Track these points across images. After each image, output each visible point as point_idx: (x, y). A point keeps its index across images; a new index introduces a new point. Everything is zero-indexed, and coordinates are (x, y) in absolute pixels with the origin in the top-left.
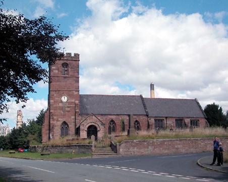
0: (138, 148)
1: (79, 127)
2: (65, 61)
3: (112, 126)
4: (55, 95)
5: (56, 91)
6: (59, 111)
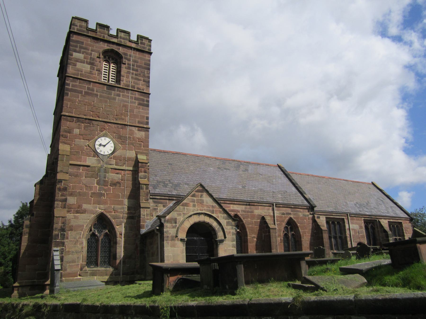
2: (115, 47)
4: (77, 131)
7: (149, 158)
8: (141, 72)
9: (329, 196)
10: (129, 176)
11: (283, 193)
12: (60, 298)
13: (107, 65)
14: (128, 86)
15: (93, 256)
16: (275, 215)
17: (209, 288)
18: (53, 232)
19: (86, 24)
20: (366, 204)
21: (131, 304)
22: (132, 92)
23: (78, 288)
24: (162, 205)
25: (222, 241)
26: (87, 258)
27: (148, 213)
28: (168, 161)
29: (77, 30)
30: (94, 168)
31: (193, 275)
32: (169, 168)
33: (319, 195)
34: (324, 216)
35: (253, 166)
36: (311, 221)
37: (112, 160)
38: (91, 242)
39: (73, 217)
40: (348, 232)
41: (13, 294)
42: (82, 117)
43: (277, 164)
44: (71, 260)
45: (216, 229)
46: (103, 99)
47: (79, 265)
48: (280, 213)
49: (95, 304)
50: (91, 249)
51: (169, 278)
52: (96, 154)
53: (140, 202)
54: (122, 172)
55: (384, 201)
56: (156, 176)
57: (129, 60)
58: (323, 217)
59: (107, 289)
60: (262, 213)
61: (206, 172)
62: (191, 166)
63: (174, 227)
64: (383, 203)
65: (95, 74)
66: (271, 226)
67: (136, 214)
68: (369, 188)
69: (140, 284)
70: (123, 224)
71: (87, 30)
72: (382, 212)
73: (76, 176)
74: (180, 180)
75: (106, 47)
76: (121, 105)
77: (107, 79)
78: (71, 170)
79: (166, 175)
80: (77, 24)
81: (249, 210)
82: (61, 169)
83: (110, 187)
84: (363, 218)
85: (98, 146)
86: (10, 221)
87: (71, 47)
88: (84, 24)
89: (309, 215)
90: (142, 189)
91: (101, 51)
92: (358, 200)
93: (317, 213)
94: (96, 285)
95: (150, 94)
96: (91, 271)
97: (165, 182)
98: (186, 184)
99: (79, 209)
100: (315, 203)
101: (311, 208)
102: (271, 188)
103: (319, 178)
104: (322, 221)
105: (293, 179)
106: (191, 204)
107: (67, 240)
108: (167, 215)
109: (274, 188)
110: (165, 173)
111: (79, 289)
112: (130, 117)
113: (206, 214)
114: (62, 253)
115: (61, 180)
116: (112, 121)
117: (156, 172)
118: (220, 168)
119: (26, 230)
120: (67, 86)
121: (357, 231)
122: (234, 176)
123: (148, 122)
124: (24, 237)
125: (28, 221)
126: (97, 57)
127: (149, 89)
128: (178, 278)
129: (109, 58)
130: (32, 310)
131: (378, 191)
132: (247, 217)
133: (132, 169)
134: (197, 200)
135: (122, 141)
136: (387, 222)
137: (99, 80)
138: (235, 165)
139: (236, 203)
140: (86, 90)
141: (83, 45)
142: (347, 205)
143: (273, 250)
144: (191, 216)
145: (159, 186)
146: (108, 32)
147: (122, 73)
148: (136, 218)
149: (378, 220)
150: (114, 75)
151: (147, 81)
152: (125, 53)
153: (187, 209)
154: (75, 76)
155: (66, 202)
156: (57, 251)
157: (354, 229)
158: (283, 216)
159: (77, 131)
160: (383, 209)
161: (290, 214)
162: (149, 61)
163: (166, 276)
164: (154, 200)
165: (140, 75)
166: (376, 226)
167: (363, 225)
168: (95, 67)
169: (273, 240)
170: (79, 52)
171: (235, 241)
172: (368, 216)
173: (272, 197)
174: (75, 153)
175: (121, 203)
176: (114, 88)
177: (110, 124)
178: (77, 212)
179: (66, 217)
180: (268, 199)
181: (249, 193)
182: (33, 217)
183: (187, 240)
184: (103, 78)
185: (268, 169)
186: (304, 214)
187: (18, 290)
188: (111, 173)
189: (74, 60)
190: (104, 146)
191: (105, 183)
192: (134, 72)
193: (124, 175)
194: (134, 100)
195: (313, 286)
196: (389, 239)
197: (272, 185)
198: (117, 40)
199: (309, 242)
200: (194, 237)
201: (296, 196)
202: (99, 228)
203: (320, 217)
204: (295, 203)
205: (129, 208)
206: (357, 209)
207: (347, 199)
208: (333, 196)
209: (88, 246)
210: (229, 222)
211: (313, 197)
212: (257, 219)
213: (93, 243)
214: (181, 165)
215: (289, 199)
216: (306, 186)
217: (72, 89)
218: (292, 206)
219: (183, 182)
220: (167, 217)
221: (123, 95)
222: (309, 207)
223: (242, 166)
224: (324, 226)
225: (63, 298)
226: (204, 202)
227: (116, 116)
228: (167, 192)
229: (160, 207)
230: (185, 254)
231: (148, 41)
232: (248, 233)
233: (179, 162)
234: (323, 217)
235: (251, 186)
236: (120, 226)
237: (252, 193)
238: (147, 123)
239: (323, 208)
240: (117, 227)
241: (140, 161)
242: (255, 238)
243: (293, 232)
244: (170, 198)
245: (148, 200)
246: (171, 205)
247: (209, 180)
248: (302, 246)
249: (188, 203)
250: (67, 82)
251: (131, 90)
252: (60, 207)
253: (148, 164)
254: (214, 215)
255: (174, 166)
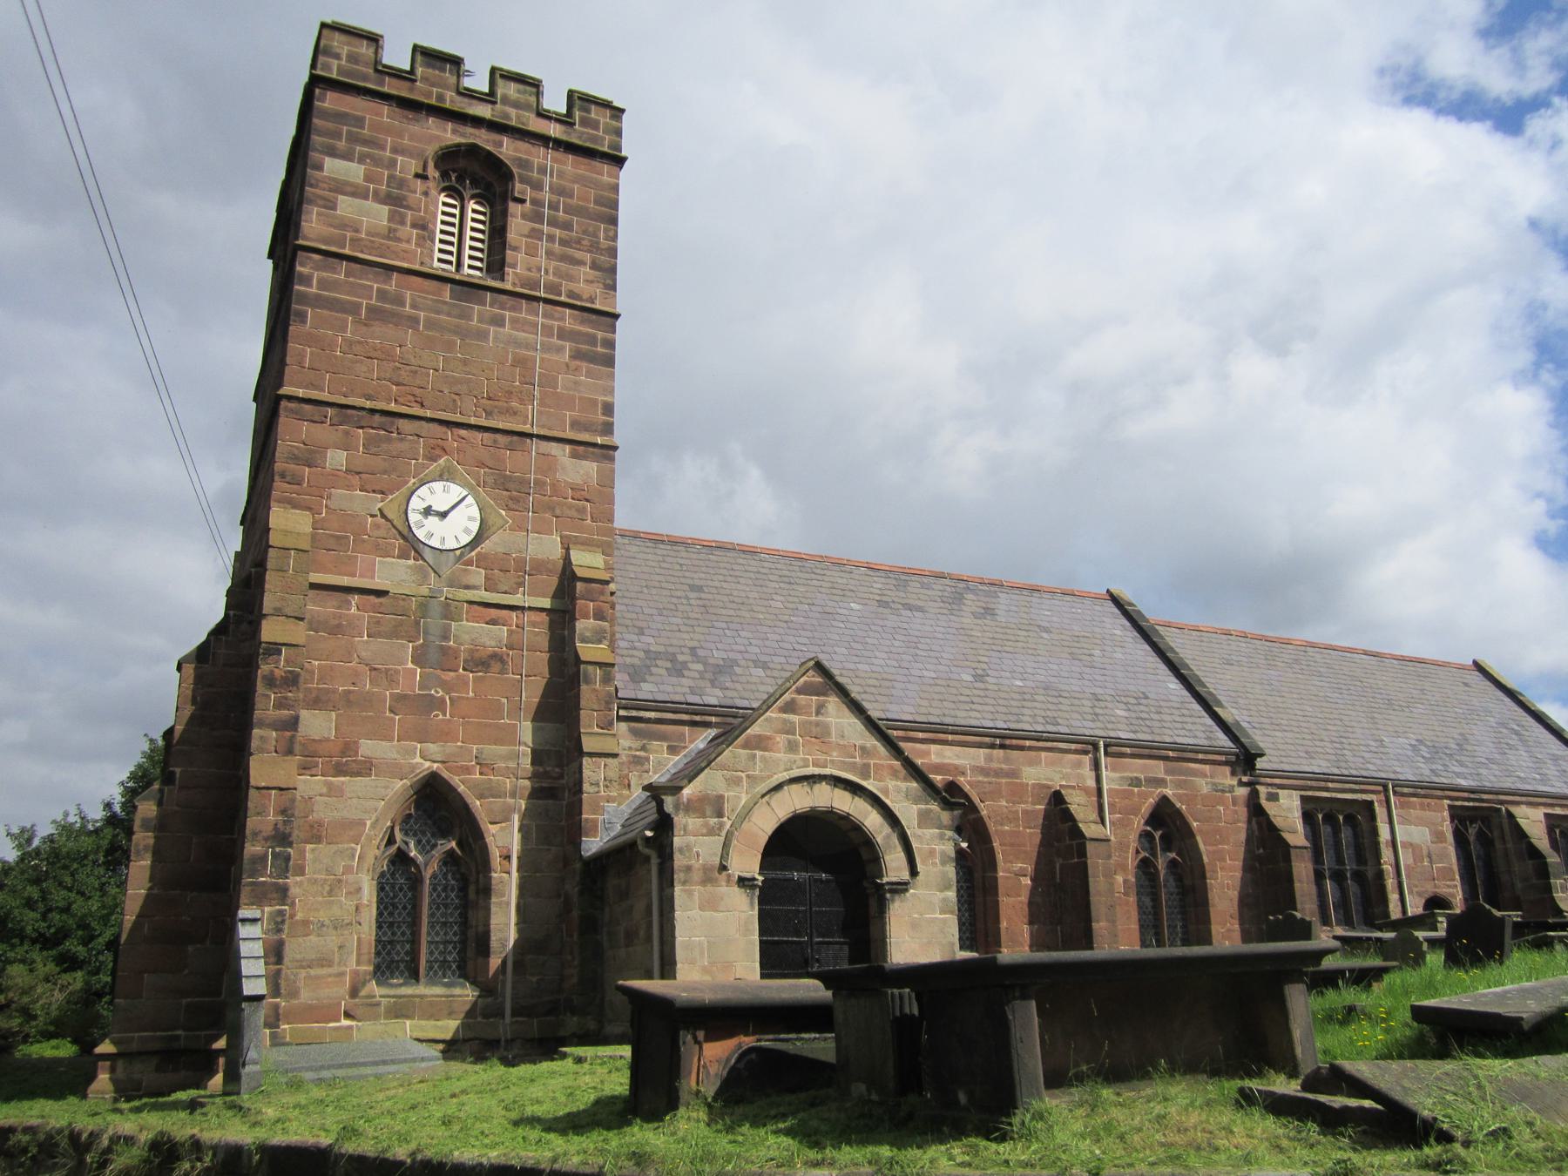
2: (483, 139)
4: (337, 458)
7: (615, 566)
8: (585, 232)
9: (1310, 714)
10: (537, 632)
11: (1133, 701)
12: (259, 1112)
13: (454, 206)
14: (536, 286)
15: (398, 942)
16: (1105, 787)
17: (874, 1097)
18: (243, 848)
19: (371, 51)
20: (1458, 745)
21: (538, 1162)
22: (549, 307)
23: (334, 1071)
24: (665, 745)
25: (900, 888)
26: (376, 946)
27: (613, 774)
28: (687, 574)
29: (340, 71)
30: (404, 600)
31: (804, 1035)
32: (693, 602)
33: (1272, 710)
34: (1294, 792)
35: (1014, 597)
36: (1246, 809)
37: (474, 568)
38: (393, 886)
39: (324, 790)
40: (1386, 855)
41: (94, 1086)
42: (356, 404)
43: (1108, 591)
44: (314, 957)
45: (879, 839)
46: (438, 335)
47: (343, 974)
48: (1123, 778)
49: (389, 1155)
50: (391, 914)
51: (701, 1048)
52: (412, 546)
53: (580, 733)
54: (512, 618)
55: (1527, 734)
56: (641, 632)
57: (538, 186)
58: (1291, 796)
59: (447, 1079)
60: (1052, 780)
61: (835, 620)
62: (775, 597)
63: (711, 832)
64: (1524, 742)
65: (408, 241)
66: (1090, 830)
67: (566, 777)
68: (1466, 685)
69: (579, 1060)
70: (516, 818)
71: (376, 70)
72: (1519, 777)
73: (336, 630)
74: (734, 647)
75: (450, 134)
76: (507, 360)
77: (453, 259)
78: (319, 607)
79: (679, 631)
80: (338, 51)
81: (1003, 766)
82: (278, 605)
83: (464, 675)
84: (1447, 802)
85: (420, 517)
86: (108, 806)
87: (317, 138)
88: (367, 49)
89: (1236, 789)
90: (587, 682)
91: (431, 150)
92: (1425, 732)
93: (1269, 780)
94: (405, 1061)
95: (616, 316)
96: (392, 1000)
97: (674, 654)
98: (757, 663)
99: (344, 760)
100: (1258, 738)
101: (1245, 759)
102: (1087, 683)
103: (1267, 643)
104: (1287, 811)
105: (1172, 650)
106: (778, 739)
107: (298, 879)
108: (686, 781)
109: (1097, 684)
110: (674, 620)
111: (340, 1073)
112: (542, 404)
113: (837, 782)
114: (279, 931)
115: (276, 644)
116: (473, 421)
117: (641, 617)
118: (887, 603)
119: (143, 838)
120: (300, 285)
121: (1425, 852)
122: (940, 636)
123: (612, 424)
124: (138, 863)
125: (151, 803)
126: (417, 176)
127: (615, 296)
128: (740, 1044)
129: (460, 179)
130: (147, 1161)
131: (1500, 694)
132: (995, 794)
133: (549, 607)
134: (803, 724)
135: (511, 498)
136: (1542, 818)
137: (422, 263)
138: (946, 594)
139: (950, 737)
140: (373, 302)
141: (362, 127)
142: (1382, 750)
143: (1098, 922)
144: (778, 788)
145: (654, 670)
146: (455, 77)
147: (512, 236)
148: (566, 794)
149: (1507, 811)
150: (479, 245)
151: (607, 266)
152: (520, 159)
153: (763, 759)
154: (333, 249)
155: (296, 730)
156: (254, 921)
157: (1411, 844)
158: (1136, 789)
159: (337, 458)
160: (1524, 764)
161: (1160, 782)
162: (615, 188)
163: (689, 1037)
164: (633, 724)
165: (579, 242)
166: (1496, 833)
167: (1447, 828)
168: (407, 214)
169: (1097, 884)
170: (347, 157)
171: (955, 888)
172: (1466, 795)
173: (1090, 717)
174: (332, 543)
175: (508, 736)
176: (481, 292)
177: (463, 432)
178: (340, 770)
179: (295, 789)
180: (1075, 723)
181: (1001, 702)
182: (171, 787)
183: (763, 882)
184: (437, 255)
185: (1074, 610)
186: (1214, 784)
187: (113, 1070)
188: (467, 620)
189: (325, 185)
190: (443, 515)
191: (447, 658)
192: (557, 232)
193: (517, 626)
194: (555, 340)
195: (1367, 1103)
196: (1550, 883)
197: (1087, 670)
198: (493, 109)
199: (1236, 893)
200: (791, 869)
201: (1185, 712)
202: (424, 833)
203: (1277, 794)
204: (1179, 740)
205: (537, 757)
206: (1422, 765)
207: (1382, 727)
208: (1327, 715)
209: (380, 901)
210: (931, 811)
211: (1248, 719)
212: (1034, 803)
213: (401, 890)
214: (735, 593)
215: (1157, 724)
216: (1218, 676)
217: (318, 297)
218: (1171, 754)
219: (746, 656)
220: (686, 792)
221: (514, 321)
222: (1237, 755)
223: (970, 596)
224: (1296, 835)
225: (270, 1112)
226: (829, 734)
227: (491, 402)
228: (684, 694)
229: (656, 752)
230: (756, 938)
231: (608, 112)
232: (999, 857)
233: (729, 579)
234: (1290, 796)
235: (1008, 674)
236: (503, 825)
237: (1013, 699)
238: (608, 429)
239: (1293, 760)
240: (493, 829)
241: (580, 573)
242: (1025, 876)
243: (1173, 855)
244: (698, 718)
245: (611, 724)
246: (700, 744)
247: (845, 651)
248: (1211, 909)
249: (769, 738)
250: (299, 268)
251: (547, 301)
252: (273, 748)
253: (612, 587)
254: (864, 783)
255: (710, 597)
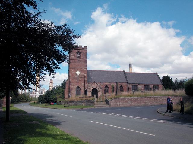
0: (122, 102)
1: (87, 89)
2: (79, 51)
3: (106, 89)
5: (73, 68)
6: (75, 80)
